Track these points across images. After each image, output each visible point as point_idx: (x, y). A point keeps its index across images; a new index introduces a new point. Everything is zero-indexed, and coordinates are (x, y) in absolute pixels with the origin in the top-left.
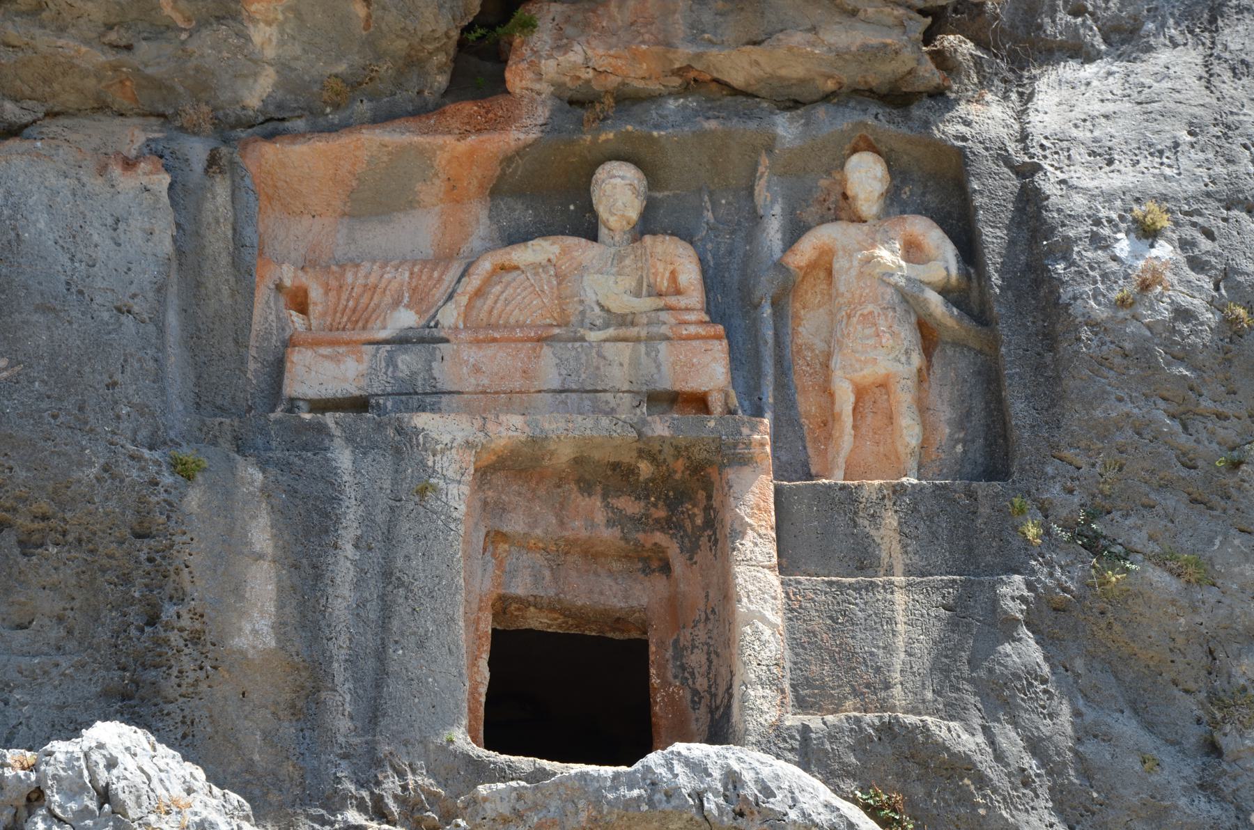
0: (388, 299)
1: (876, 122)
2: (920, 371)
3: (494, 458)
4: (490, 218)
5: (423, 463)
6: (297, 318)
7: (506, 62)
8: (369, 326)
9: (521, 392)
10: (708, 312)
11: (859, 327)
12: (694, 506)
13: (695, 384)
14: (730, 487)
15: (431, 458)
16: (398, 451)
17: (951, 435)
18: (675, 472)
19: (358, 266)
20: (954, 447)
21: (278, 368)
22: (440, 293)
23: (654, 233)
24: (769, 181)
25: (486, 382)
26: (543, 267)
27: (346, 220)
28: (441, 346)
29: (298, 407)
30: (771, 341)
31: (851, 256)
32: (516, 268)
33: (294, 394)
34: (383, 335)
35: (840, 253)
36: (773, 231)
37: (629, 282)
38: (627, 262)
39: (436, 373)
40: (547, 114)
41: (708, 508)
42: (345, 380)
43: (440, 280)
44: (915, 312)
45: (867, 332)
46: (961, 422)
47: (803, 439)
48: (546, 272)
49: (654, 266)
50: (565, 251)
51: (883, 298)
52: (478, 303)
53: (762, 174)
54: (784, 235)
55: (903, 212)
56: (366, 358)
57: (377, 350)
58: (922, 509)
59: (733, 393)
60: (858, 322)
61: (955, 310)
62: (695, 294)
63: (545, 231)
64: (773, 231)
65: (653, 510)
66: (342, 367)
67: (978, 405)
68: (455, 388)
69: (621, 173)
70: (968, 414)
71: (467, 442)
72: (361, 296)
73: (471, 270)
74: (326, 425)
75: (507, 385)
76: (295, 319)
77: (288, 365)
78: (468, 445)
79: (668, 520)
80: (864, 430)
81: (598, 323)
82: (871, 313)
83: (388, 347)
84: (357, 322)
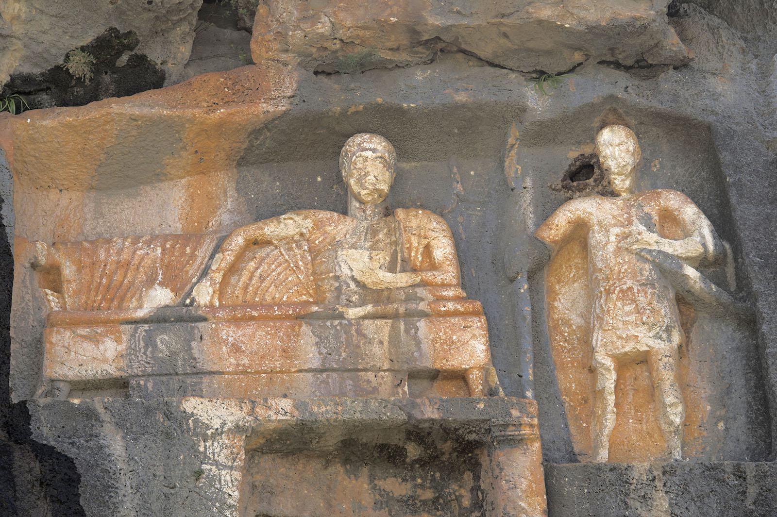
0: (142, 277)
1: (626, 96)
2: (680, 347)
3: (262, 441)
4: (237, 190)
5: (194, 448)
6: (52, 297)
7: (249, 31)
8: (125, 305)
9: (282, 372)
10: (464, 287)
11: (619, 304)
12: (461, 487)
13: (456, 361)
14: (502, 470)
15: (202, 444)
16: (168, 435)
17: (712, 412)
18: (443, 454)
19: (109, 241)
20: (716, 424)
21: (38, 347)
22: (193, 270)
23: (405, 207)
24: (518, 154)
25: (246, 361)
26: (296, 242)
27: (93, 194)
28: (201, 325)
29: (58, 389)
30: (529, 318)
31: (607, 231)
32: (269, 243)
33: (55, 376)
34: (140, 314)
35: (596, 228)
36: (526, 204)
37: (383, 257)
38: (381, 236)
39: (196, 353)
40: (295, 86)
41: (475, 489)
42: (105, 361)
43: (193, 256)
44: (673, 287)
45: (627, 308)
46: (722, 399)
47: (563, 416)
48: (299, 247)
49: (409, 241)
50: (318, 225)
51: (642, 275)
52: (233, 280)
53: (513, 146)
54: (536, 207)
55: (654, 186)
56: (124, 338)
57: (136, 330)
58: (692, 489)
59: (493, 371)
60: (618, 299)
61: (713, 286)
62: (450, 269)
63: (296, 206)
64: (526, 204)
65: (419, 491)
66: (101, 347)
67: (739, 382)
68: (215, 368)
69: (372, 146)
70: (728, 391)
71: (237, 426)
72: (114, 273)
73: (225, 246)
74: (95, 409)
75: (267, 365)
76: (51, 298)
77: (48, 345)
78: (238, 429)
79: (435, 501)
80: (626, 407)
81: (354, 299)
82: (630, 289)
83: (146, 327)
84: (112, 300)
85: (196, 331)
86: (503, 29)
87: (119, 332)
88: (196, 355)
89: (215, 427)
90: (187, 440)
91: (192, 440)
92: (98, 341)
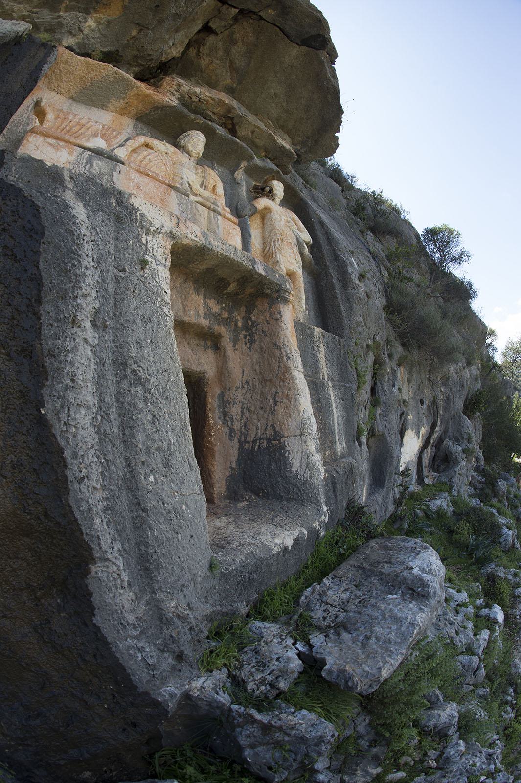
5: (137, 237)
15: (144, 236)
28: (121, 165)
34: (90, 145)
50: (174, 153)
52: (135, 155)
57: (83, 152)
66: (59, 153)
83: (90, 153)
85: (118, 167)
87: (73, 149)
88: (115, 180)
90: (134, 228)
91: (138, 230)
92: (58, 149)
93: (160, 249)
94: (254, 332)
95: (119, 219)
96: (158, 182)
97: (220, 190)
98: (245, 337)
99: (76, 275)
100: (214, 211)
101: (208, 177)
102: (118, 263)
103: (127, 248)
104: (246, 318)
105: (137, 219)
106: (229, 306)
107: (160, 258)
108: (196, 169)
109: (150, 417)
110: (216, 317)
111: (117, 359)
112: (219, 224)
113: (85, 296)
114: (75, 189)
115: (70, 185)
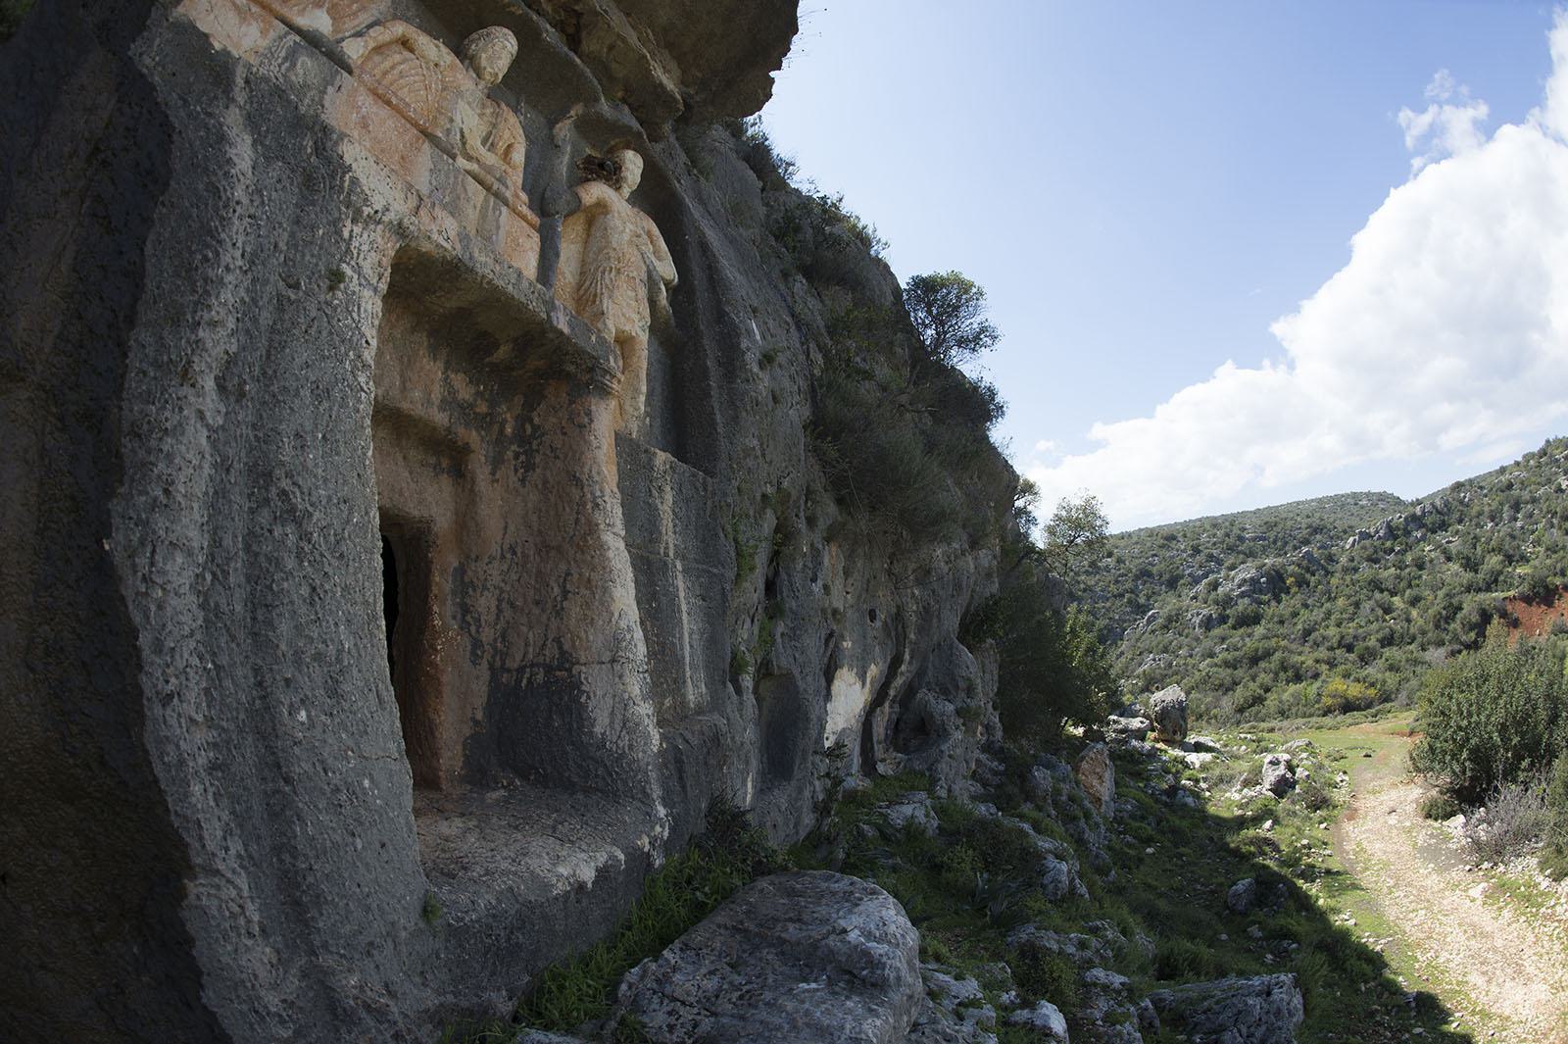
5: (335, 225)
15: (348, 223)
71: (400, 224)
83: (298, 39)
86: (619, 43)
89: (376, 208)
91: (340, 210)
93: (373, 254)
94: (534, 447)
95: (309, 182)
96: (403, 121)
97: (519, 156)
98: (517, 456)
99: (206, 280)
100: (497, 195)
101: (501, 126)
102: (289, 270)
103: (311, 243)
104: (523, 420)
105: (342, 187)
106: (492, 391)
107: (370, 272)
108: (484, 106)
109: (305, 591)
110: (464, 410)
111: (256, 464)
112: (502, 223)
113: (213, 324)
114: (248, 107)
115: (241, 98)
